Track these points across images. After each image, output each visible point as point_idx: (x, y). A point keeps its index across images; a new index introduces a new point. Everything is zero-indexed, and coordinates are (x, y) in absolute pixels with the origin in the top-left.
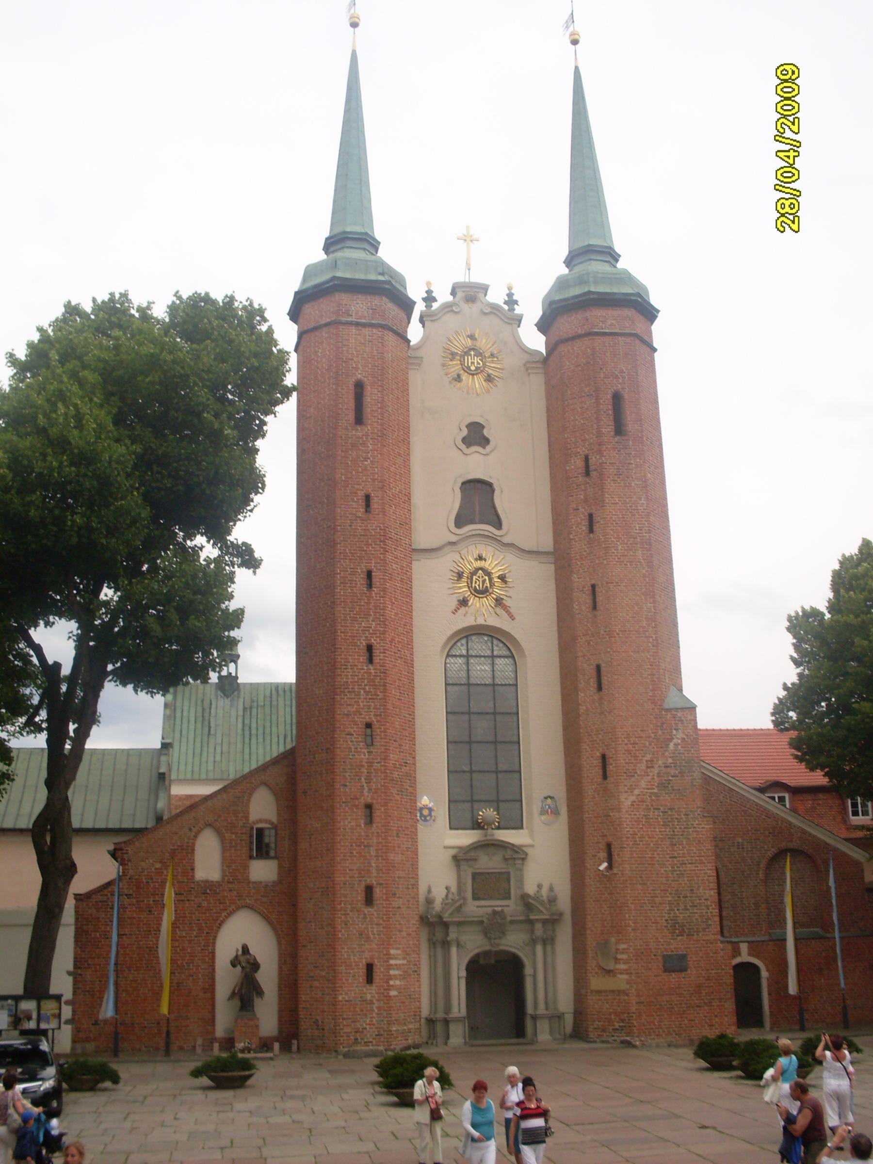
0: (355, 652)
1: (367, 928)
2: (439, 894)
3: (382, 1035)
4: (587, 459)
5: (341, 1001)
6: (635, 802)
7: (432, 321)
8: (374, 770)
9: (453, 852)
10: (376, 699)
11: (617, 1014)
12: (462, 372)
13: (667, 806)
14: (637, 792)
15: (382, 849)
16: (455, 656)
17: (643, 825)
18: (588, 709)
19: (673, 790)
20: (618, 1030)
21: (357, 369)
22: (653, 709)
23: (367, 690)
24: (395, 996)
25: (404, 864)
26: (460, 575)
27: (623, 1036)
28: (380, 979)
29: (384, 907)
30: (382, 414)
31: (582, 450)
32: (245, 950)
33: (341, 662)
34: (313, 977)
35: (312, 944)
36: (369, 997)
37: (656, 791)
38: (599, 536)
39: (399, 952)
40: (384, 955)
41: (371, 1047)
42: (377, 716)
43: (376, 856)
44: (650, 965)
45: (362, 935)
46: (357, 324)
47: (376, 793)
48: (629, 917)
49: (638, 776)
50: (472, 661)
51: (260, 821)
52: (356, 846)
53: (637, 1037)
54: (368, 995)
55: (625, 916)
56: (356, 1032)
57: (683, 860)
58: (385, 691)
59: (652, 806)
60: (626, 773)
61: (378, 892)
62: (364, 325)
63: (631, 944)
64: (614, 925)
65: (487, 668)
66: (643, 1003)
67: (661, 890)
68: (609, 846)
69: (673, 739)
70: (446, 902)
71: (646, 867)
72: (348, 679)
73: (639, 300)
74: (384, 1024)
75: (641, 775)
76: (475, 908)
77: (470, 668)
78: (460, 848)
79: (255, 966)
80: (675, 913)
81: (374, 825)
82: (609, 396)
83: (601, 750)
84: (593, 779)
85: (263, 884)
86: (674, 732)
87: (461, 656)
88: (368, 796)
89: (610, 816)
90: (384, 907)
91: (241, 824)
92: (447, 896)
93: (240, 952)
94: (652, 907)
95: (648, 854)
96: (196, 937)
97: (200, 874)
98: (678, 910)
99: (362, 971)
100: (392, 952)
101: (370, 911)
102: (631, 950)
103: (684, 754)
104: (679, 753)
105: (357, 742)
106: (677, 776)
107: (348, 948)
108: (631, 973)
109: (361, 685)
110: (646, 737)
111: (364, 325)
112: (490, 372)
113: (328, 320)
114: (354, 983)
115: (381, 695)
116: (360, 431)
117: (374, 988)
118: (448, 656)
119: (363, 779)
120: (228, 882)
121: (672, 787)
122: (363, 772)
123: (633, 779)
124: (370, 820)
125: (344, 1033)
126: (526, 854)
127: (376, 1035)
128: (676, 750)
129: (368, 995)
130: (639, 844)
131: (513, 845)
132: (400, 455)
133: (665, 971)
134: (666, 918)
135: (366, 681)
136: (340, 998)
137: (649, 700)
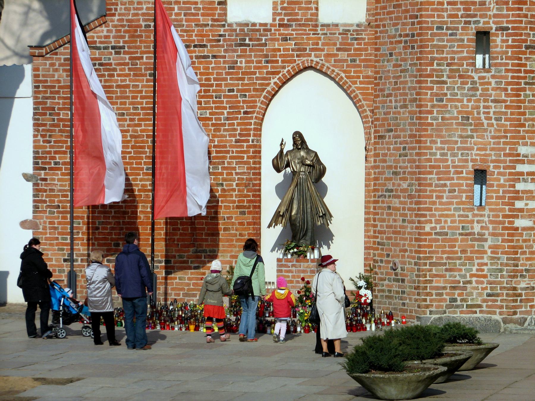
1: (478, 107)
3: (498, 295)
5: (429, 234)
24: (524, 229)
28: (498, 198)
29: (507, 71)
34: (392, 191)
35: (391, 134)
36: (477, 228)
40: (505, 155)
41: (478, 315)
54: (475, 224)
74: (502, 277)
85: (341, 29)
90: (507, 71)
93: (289, 146)
96: (227, 119)
100: (522, 150)
101: (484, 78)
107: (442, 142)
114: (452, 203)
120: (280, 26)
125: (432, 288)
127: (489, 295)
129: (475, 224)
136: (427, 229)
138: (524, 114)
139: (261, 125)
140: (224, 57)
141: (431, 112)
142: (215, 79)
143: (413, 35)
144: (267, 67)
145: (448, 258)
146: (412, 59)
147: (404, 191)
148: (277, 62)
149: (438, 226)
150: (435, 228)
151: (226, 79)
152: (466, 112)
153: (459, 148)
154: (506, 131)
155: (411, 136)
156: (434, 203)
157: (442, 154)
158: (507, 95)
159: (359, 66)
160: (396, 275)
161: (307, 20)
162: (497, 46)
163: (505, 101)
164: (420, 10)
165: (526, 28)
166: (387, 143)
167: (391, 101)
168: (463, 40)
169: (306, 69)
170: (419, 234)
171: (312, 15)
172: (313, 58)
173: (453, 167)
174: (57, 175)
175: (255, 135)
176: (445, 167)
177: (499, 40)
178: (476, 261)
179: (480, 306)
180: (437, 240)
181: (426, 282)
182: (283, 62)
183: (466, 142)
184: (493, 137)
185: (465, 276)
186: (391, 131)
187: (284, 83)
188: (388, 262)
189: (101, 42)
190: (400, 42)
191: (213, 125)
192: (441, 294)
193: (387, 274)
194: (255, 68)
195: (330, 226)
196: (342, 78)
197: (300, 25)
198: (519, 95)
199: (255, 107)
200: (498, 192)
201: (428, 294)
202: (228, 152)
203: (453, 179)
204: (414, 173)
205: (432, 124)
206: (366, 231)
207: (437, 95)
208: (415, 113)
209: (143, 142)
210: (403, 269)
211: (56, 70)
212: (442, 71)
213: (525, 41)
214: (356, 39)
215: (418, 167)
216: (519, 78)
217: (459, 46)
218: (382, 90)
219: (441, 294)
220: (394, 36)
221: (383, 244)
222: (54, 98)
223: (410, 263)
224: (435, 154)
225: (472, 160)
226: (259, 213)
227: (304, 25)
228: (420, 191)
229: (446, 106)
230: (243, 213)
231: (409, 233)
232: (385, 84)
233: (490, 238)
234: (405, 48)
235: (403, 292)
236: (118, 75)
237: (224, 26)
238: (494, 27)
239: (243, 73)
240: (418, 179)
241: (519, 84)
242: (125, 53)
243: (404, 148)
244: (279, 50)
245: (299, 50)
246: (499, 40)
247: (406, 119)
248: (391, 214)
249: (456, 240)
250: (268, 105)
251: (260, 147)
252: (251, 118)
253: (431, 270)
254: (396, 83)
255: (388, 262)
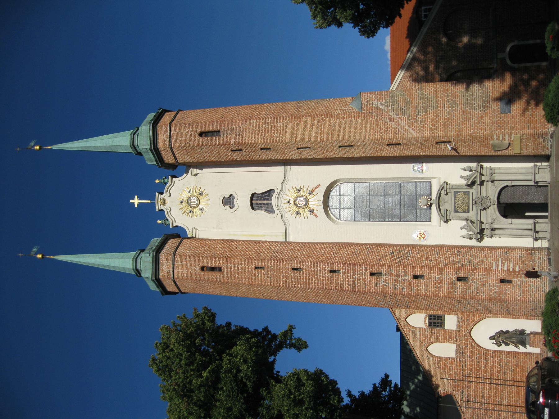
0: (334, 280)
1: (480, 281)
2: (464, 232)
4: (232, 151)
5: (521, 298)
6: (413, 128)
7: (175, 222)
8: (395, 273)
9: (442, 222)
10: (357, 269)
11: (536, 140)
12: (199, 207)
13: (415, 110)
14: (407, 128)
15: (437, 271)
16: (340, 215)
17: (426, 124)
18: (363, 152)
19: (406, 106)
20: (544, 140)
21: (195, 270)
22: (362, 118)
23: (353, 274)
24: (519, 268)
25: (446, 256)
26: (298, 213)
27: (548, 137)
28: (509, 276)
29: (469, 272)
30: (216, 258)
31: (229, 153)
32: (492, 338)
33: (339, 287)
34: (507, 309)
35: (489, 309)
36: (519, 283)
37: (407, 117)
38: (272, 146)
39: (494, 263)
41: (547, 283)
42: (366, 270)
43: (441, 275)
44: (506, 121)
45: (484, 284)
46: (174, 268)
47: (407, 272)
48: (478, 133)
49: (398, 126)
50: (342, 206)
51: (425, 322)
52: (435, 285)
53: (548, 130)
55: (478, 135)
56: (539, 291)
57: (446, 101)
58: (353, 264)
59: (415, 119)
60: (397, 134)
61: (460, 275)
62: (174, 265)
63: (494, 132)
64: (483, 141)
65: (346, 198)
66: (528, 125)
67: (463, 114)
68: (437, 143)
69: (378, 106)
70: (469, 230)
71: (450, 123)
72: (347, 283)
73: (153, 122)
75: (398, 125)
76: (474, 211)
77: (346, 208)
78: (440, 217)
79: (501, 333)
80: (477, 105)
81: (424, 274)
82: (201, 139)
83: (385, 146)
84: (401, 150)
86: (374, 105)
87: (340, 212)
88: (409, 277)
89: (421, 142)
91: (426, 333)
92: (465, 229)
93: (494, 341)
94: (472, 120)
95: (442, 121)
96: (485, 360)
97: (453, 355)
98: (475, 104)
99: (504, 285)
100: (494, 268)
101: (471, 279)
102: (497, 132)
103: (386, 100)
104: (386, 103)
105: (380, 281)
106: (399, 104)
107: (491, 293)
108: (511, 132)
109: (351, 277)
110: (377, 122)
111: (174, 265)
112: (198, 193)
113: (173, 282)
114: (511, 291)
115: (356, 267)
116: (224, 270)
117: (514, 280)
118: (340, 219)
119: (399, 279)
120: (457, 341)
121: (404, 107)
122: (396, 279)
123: (400, 129)
124: (422, 277)
126: (444, 182)
128: (384, 105)
130: (437, 126)
131: (439, 190)
132: (236, 247)
133: (511, 113)
134: (479, 111)
135: (348, 274)
136: (519, 298)
137: (357, 120)
138: (483, 267)
139: (487, 350)
140: (466, 359)
141: (482, 296)
142: (473, 363)
143: (458, 300)
144: (469, 346)
145: (529, 292)
146: (465, 301)
147: (507, 306)
148: (468, 343)
149: (518, 295)
150: (519, 296)
151: (473, 359)
152: (482, 285)
153: (493, 288)
154: (488, 273)
155: (489, 302)
156: (511, 296)
157: (495, 293)
158: (477, 272)
159: (470, 318)
160: (534, 309)
161: (455, 333)
162: (462, 275)
163: (479, 273)
164: (450, 298)
165: (456, 266)
166: (492, 310)
167: (479, 308)
168: (459, 285)
169: (470, 334)
170: (521, 301)
171: (454, 332)
172: (467, 332)
173: (499, 289)
174: (502, 415)
175: (490, 352)
176: (499, 292)
177: (459, 274)
178: (530, 283)
179: (545, 283)
180: (523, 295)
181: (536, 299)
182: (468, 341)
183: (491, 285)
184: (490, 277)
185: (535, 287)
186: (488, 309)
187: (475, 341)
188: (530, 312)
189: (460, 397)
190: (460, 305)
191: (487, 364)
192: (541, 295)
193: (534, 312)
194: (469, 350)
195: (520, 330)
196: (473, 324)
197: (457, 335)
198: (477, 269)
199: (482, 351)
200: (507, 276)
201: (541, 299)
202: (496, 360)
203: (503, 290)
204: (501, 302)
205: (485, 296)
206: (522, 319)
207: (476, 294)
208: (482, 301)
209: (492, 387)
210: (532, 307)
211: (469, 412)
212: (469, 292)
213: (460, 266)
214: (461, 319)
215: (499, 301)
216: (471, 269)
217: (461, 287)
218: (475, 311)
219: (541, 295)
220: (459, 306)
221: (525, 313)
222: (477, 413)
223: (531, 304)
224: (495, 295)
225: (497, 283)
226: (515, 352)
227: (457, 334)
228: (507, 300)
229: (480, 291)
230: (515, 357)
231: (521, 304)
232: (473, 310)
233: (522, 279)
234: (462, 303)
235: (540, 307)
236: (471, 392)
237: (456, 359)
238: (456, 276)
239: (471, 354)
240: (503, 301)
241: (473, 269)
242: (464, 390)
243: (493, 305)
244: (464, 342)
245: (464, 336)
246: (459, 274)
247: (484, 304)
248: (515, 310)
249: (523, 289)
250: (481, 347)
251: (494, 350)
252: (485, 352)
253: (533, 298)
254: (473, 306)
255: (530, 312)
